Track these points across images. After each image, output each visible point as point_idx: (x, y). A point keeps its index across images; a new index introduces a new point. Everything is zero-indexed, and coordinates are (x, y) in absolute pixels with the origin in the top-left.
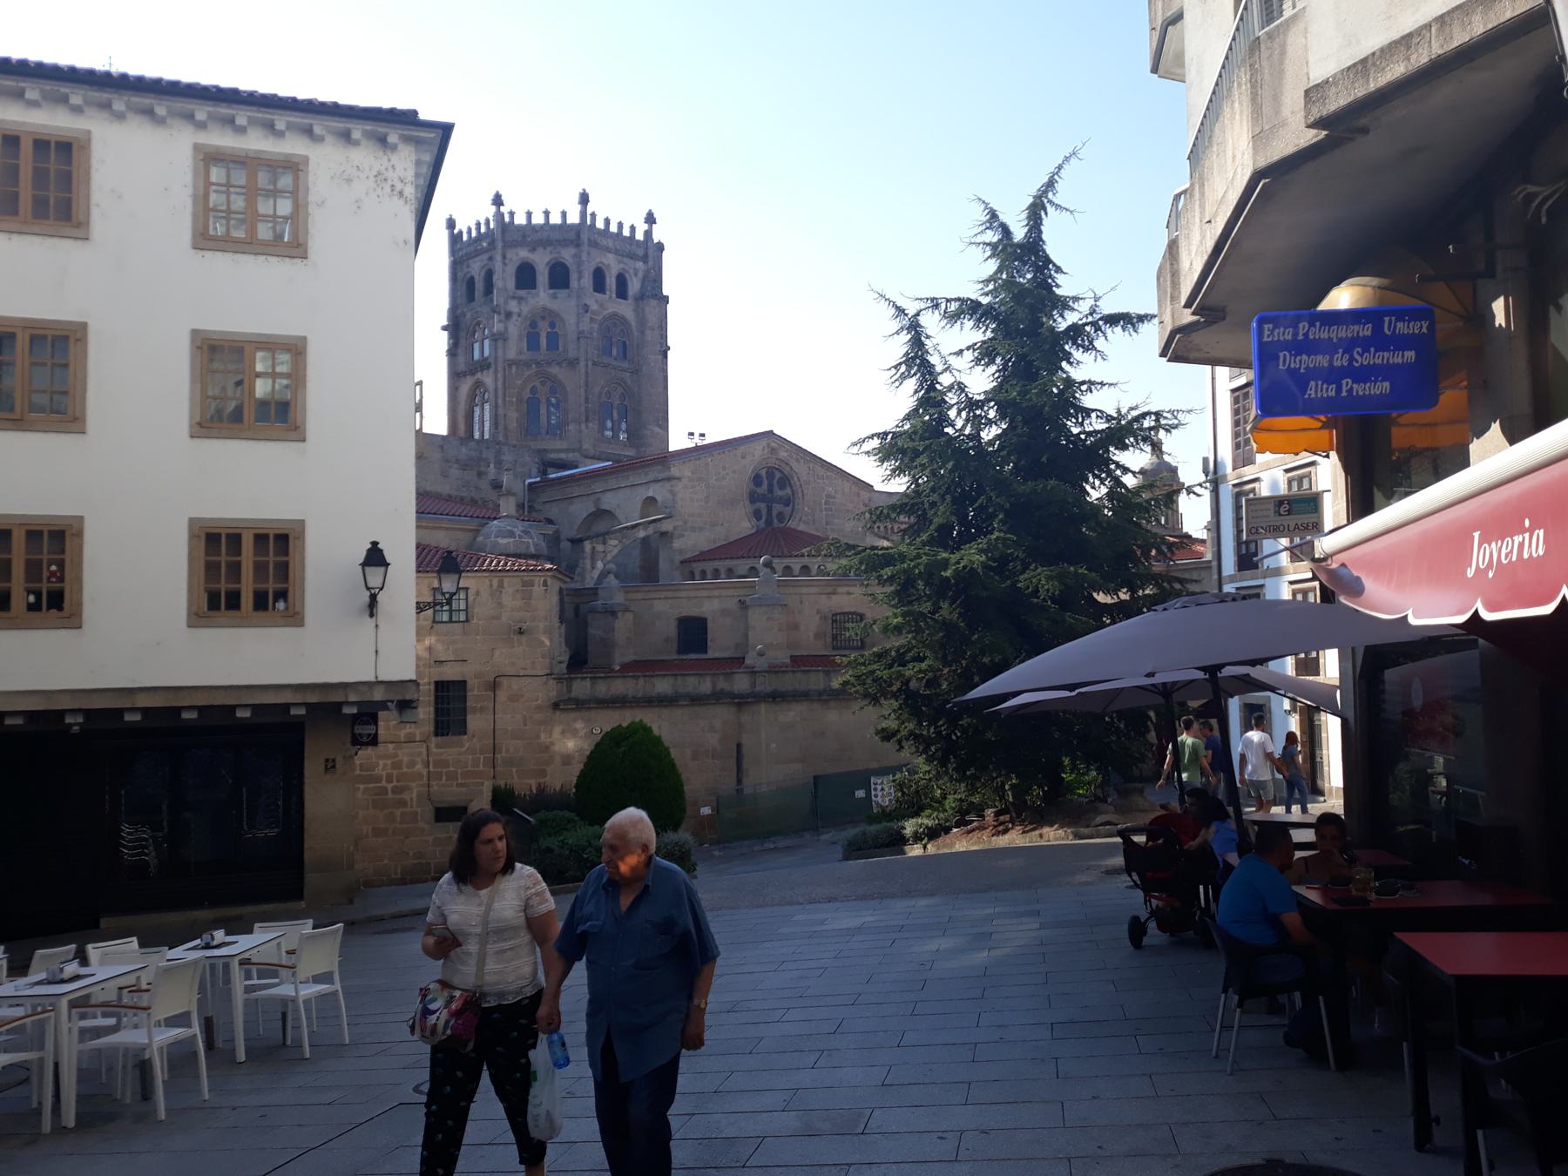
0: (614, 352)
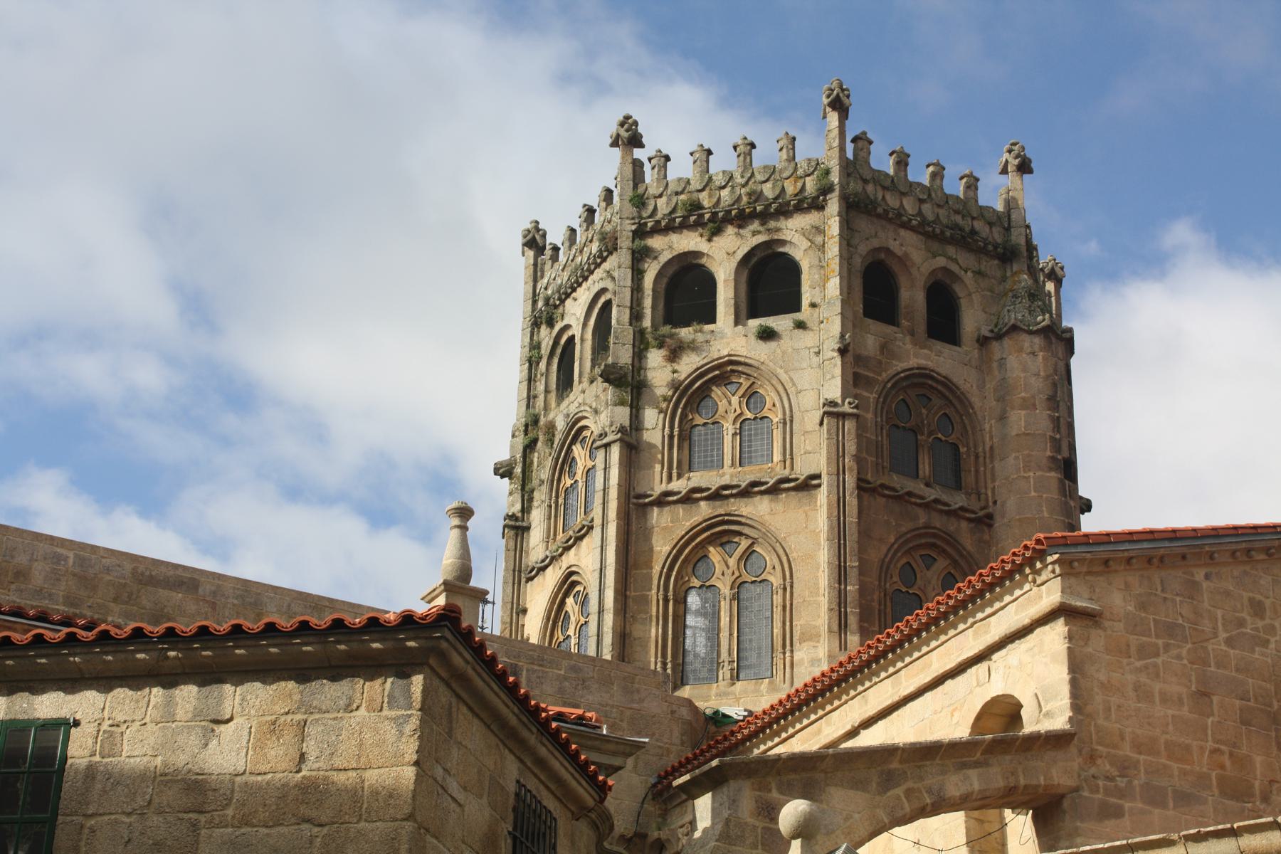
0: (925, 468)
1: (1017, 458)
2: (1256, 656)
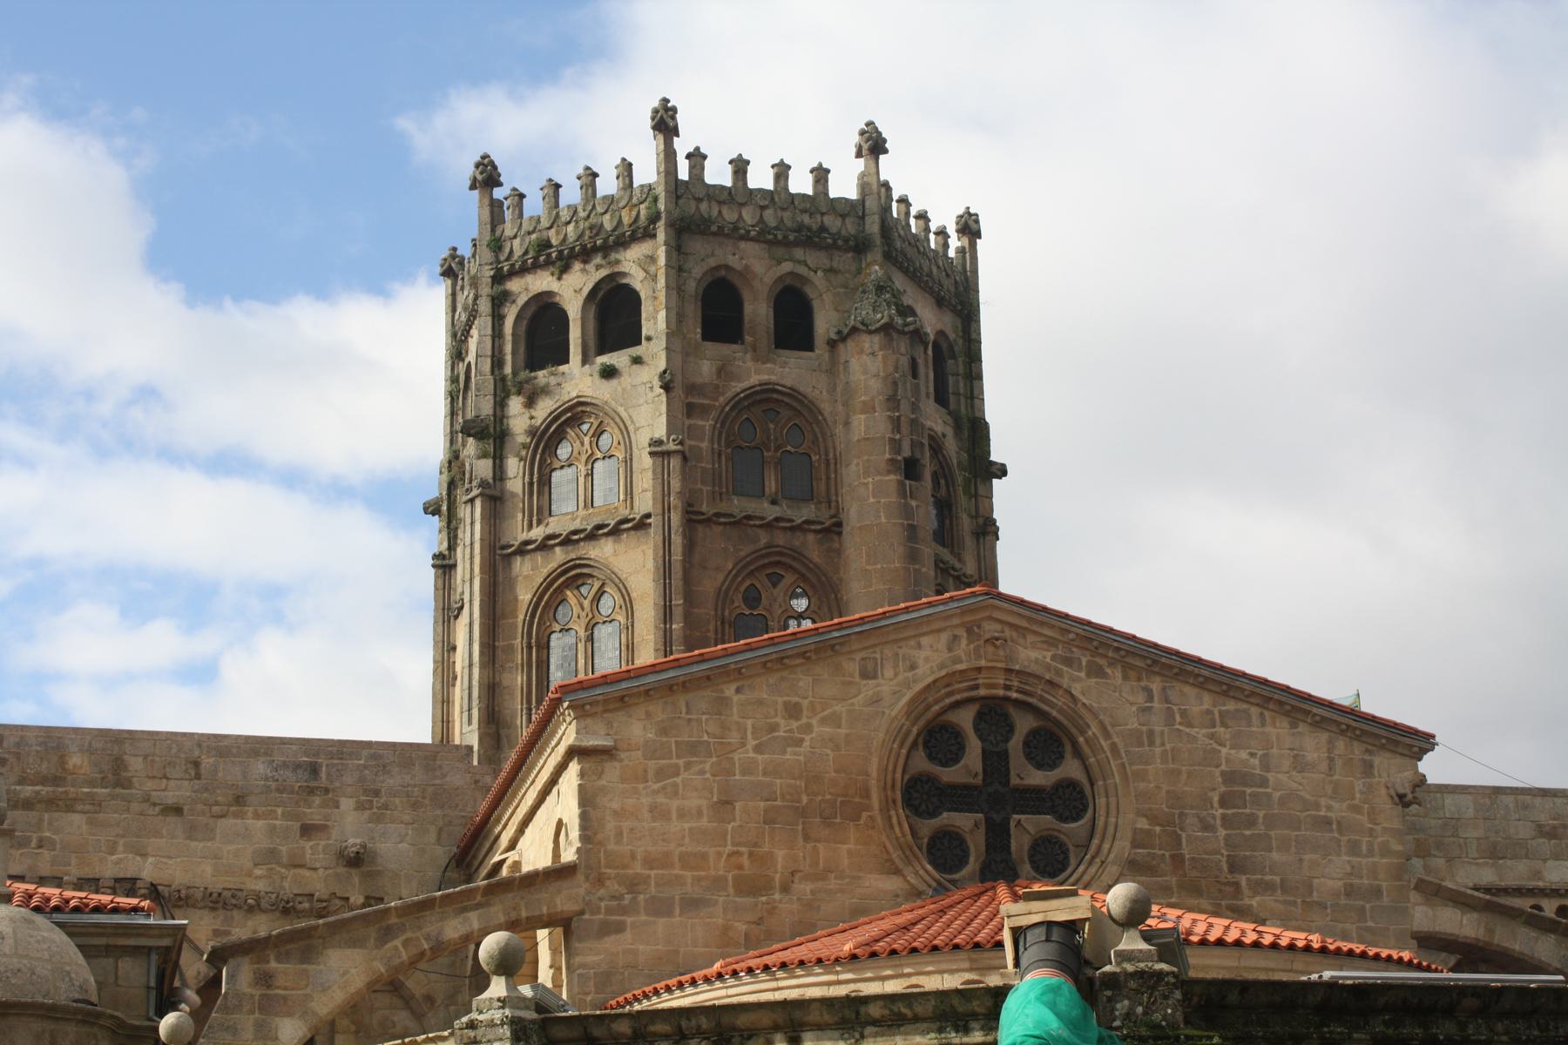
0: (771, 485)
1: (858, 464)
2: (788, 757)
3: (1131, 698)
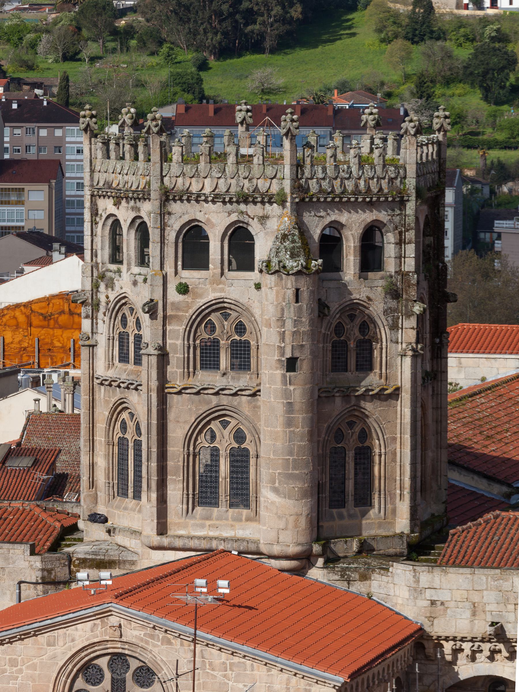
3: (184, 656)
